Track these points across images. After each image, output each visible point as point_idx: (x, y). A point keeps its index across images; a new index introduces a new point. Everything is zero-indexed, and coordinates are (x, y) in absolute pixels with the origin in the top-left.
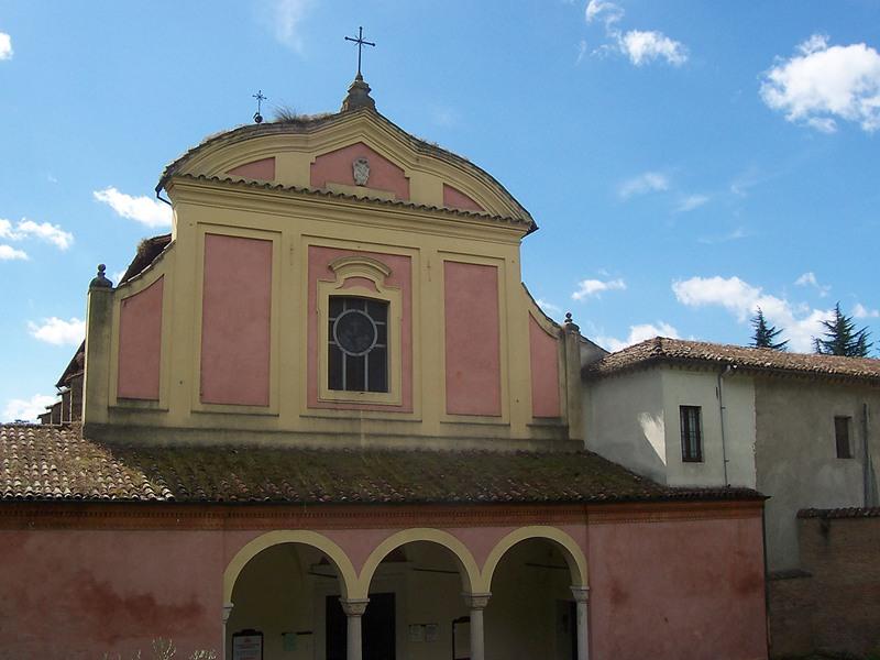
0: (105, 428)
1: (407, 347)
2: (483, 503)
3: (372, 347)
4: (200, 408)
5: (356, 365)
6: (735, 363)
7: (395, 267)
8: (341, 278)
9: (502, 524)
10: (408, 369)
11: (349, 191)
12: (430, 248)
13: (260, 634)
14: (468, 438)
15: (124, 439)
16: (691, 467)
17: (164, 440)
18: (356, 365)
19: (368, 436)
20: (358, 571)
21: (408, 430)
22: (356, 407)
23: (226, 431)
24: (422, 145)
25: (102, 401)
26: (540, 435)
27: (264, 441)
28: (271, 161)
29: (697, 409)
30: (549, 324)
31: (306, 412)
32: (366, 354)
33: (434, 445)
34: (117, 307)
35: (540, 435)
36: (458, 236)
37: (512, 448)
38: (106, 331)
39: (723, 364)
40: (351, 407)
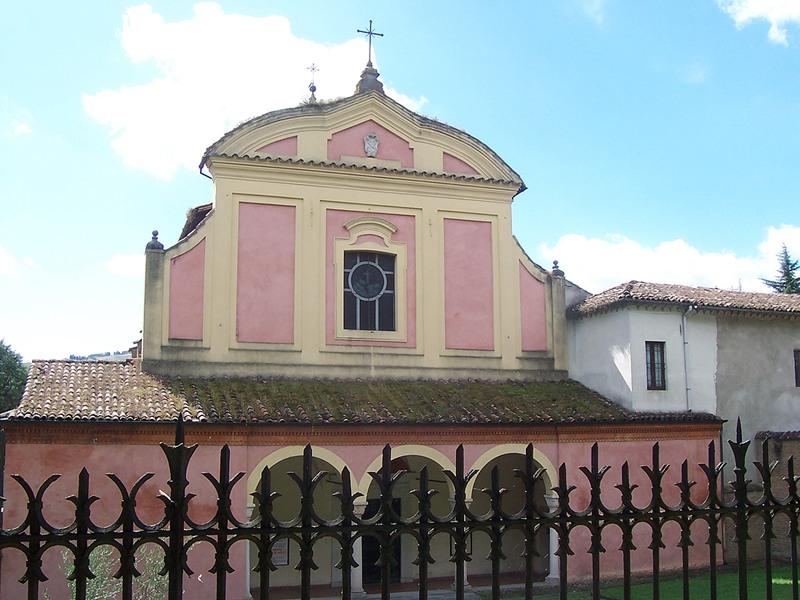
0: (160, 363)
1: (412, 293)
2: (465, 424)
3: (382, 293)
4: (236, 345)
5: (368, 308)
6: (696, 304)
7: (401, 224)
8: (354, 236)
9: (482, 442)
10: (412, 311)
11: (360, 162)
12: (431, 208)
14: (464, 369)
15: (174, 372)
16: (655, 394)
17: (206, 372)
18: (368, 308)
19: (376, 367)
21: (411, 362)
22: (367, 344)
23: (258, 364)
24: (424, 120)
25: (157, 342)
26: (528, 366)
27: (289, 372)
28: (292, 142)
29: (662, 344)
30: (537, 271)
31: (325, 348)
32: (376, 299)
33: (434, 375)
34: (167, 265)
35: (528, 366)
36: (461, 198)
37: (505, 377)
38: (159, 285)
39: (686, 304)
40: (362, 343)
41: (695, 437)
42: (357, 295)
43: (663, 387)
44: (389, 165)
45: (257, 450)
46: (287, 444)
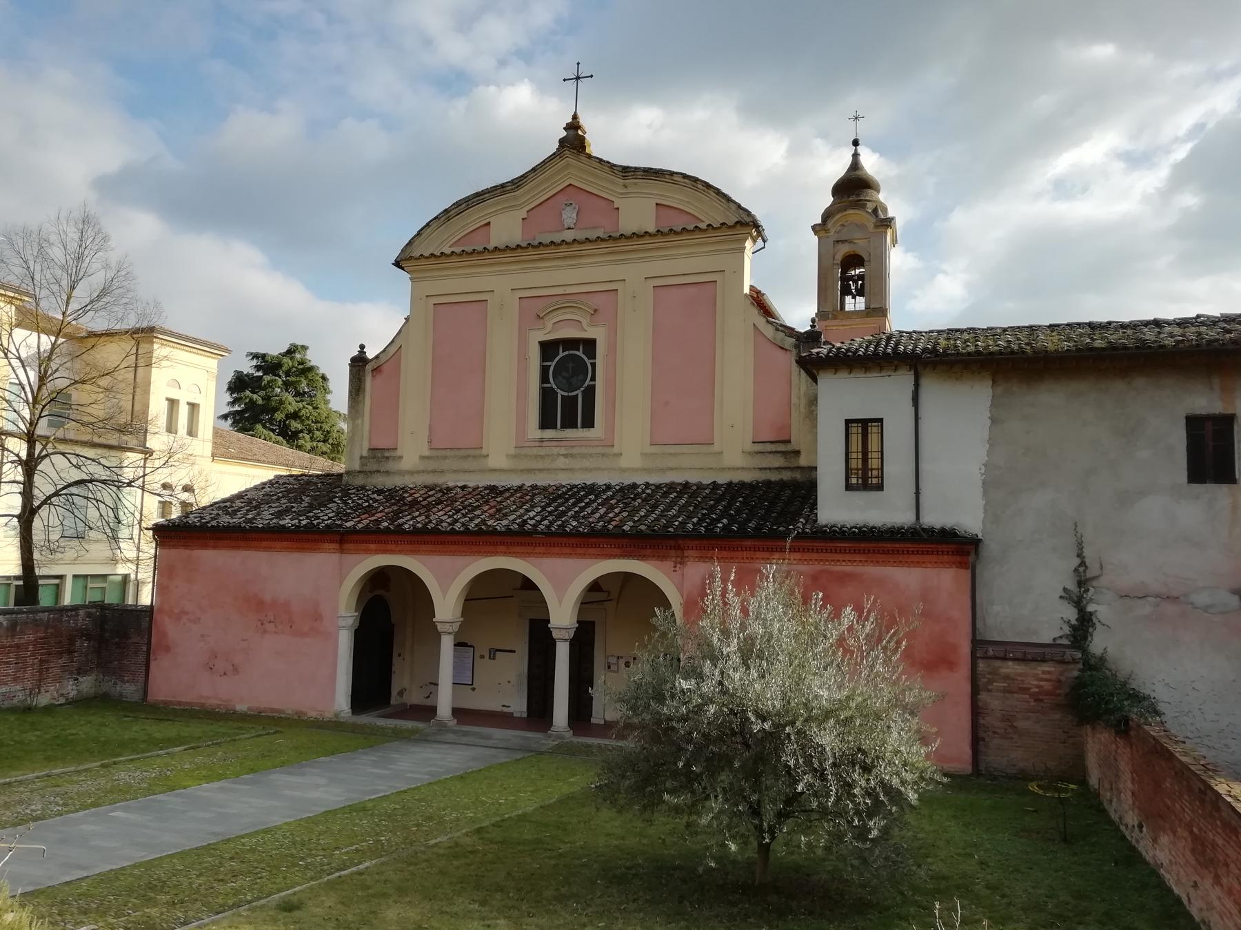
5: (570, 403)
8: (549, 324)
9: (584, 556)
13: (471, 646)
16: (860, 497)
18: (570, 403)
20: (444, 592)
24: (626, 170)
28: (487, 227)
32: (579, 393)
40: (555, 444)
41: (918, 564)
42: (559, 391)
43: (880, 487)
44: (592, 235)
45: (349, 558)
46: (377, 552)
